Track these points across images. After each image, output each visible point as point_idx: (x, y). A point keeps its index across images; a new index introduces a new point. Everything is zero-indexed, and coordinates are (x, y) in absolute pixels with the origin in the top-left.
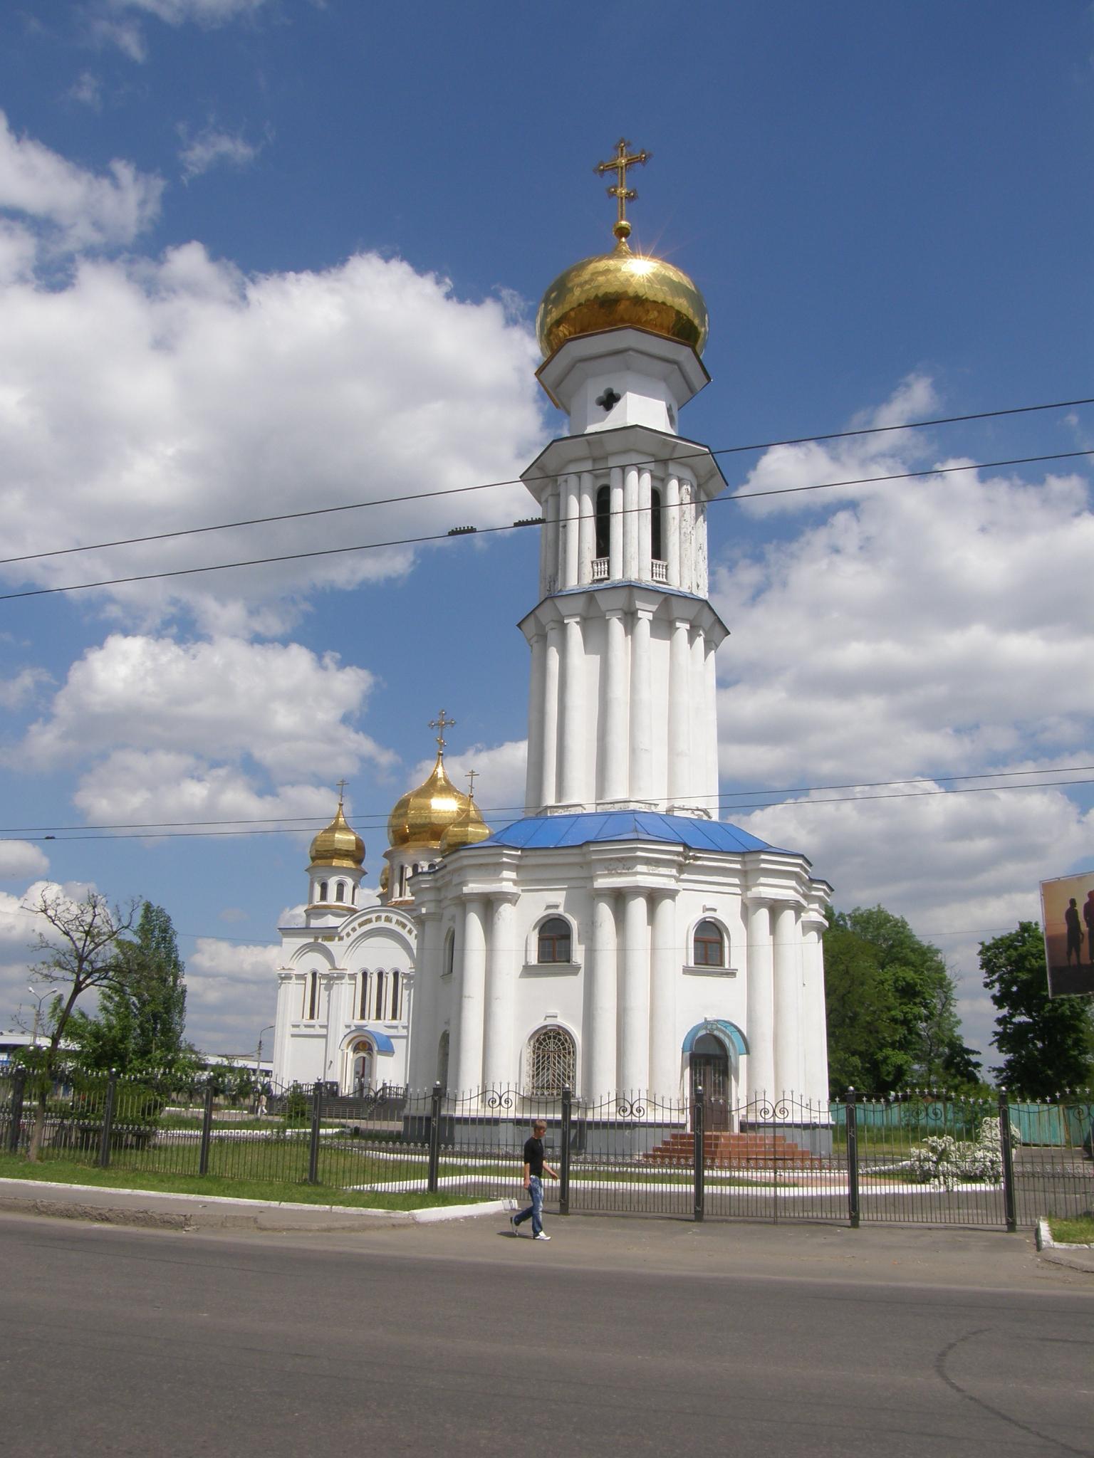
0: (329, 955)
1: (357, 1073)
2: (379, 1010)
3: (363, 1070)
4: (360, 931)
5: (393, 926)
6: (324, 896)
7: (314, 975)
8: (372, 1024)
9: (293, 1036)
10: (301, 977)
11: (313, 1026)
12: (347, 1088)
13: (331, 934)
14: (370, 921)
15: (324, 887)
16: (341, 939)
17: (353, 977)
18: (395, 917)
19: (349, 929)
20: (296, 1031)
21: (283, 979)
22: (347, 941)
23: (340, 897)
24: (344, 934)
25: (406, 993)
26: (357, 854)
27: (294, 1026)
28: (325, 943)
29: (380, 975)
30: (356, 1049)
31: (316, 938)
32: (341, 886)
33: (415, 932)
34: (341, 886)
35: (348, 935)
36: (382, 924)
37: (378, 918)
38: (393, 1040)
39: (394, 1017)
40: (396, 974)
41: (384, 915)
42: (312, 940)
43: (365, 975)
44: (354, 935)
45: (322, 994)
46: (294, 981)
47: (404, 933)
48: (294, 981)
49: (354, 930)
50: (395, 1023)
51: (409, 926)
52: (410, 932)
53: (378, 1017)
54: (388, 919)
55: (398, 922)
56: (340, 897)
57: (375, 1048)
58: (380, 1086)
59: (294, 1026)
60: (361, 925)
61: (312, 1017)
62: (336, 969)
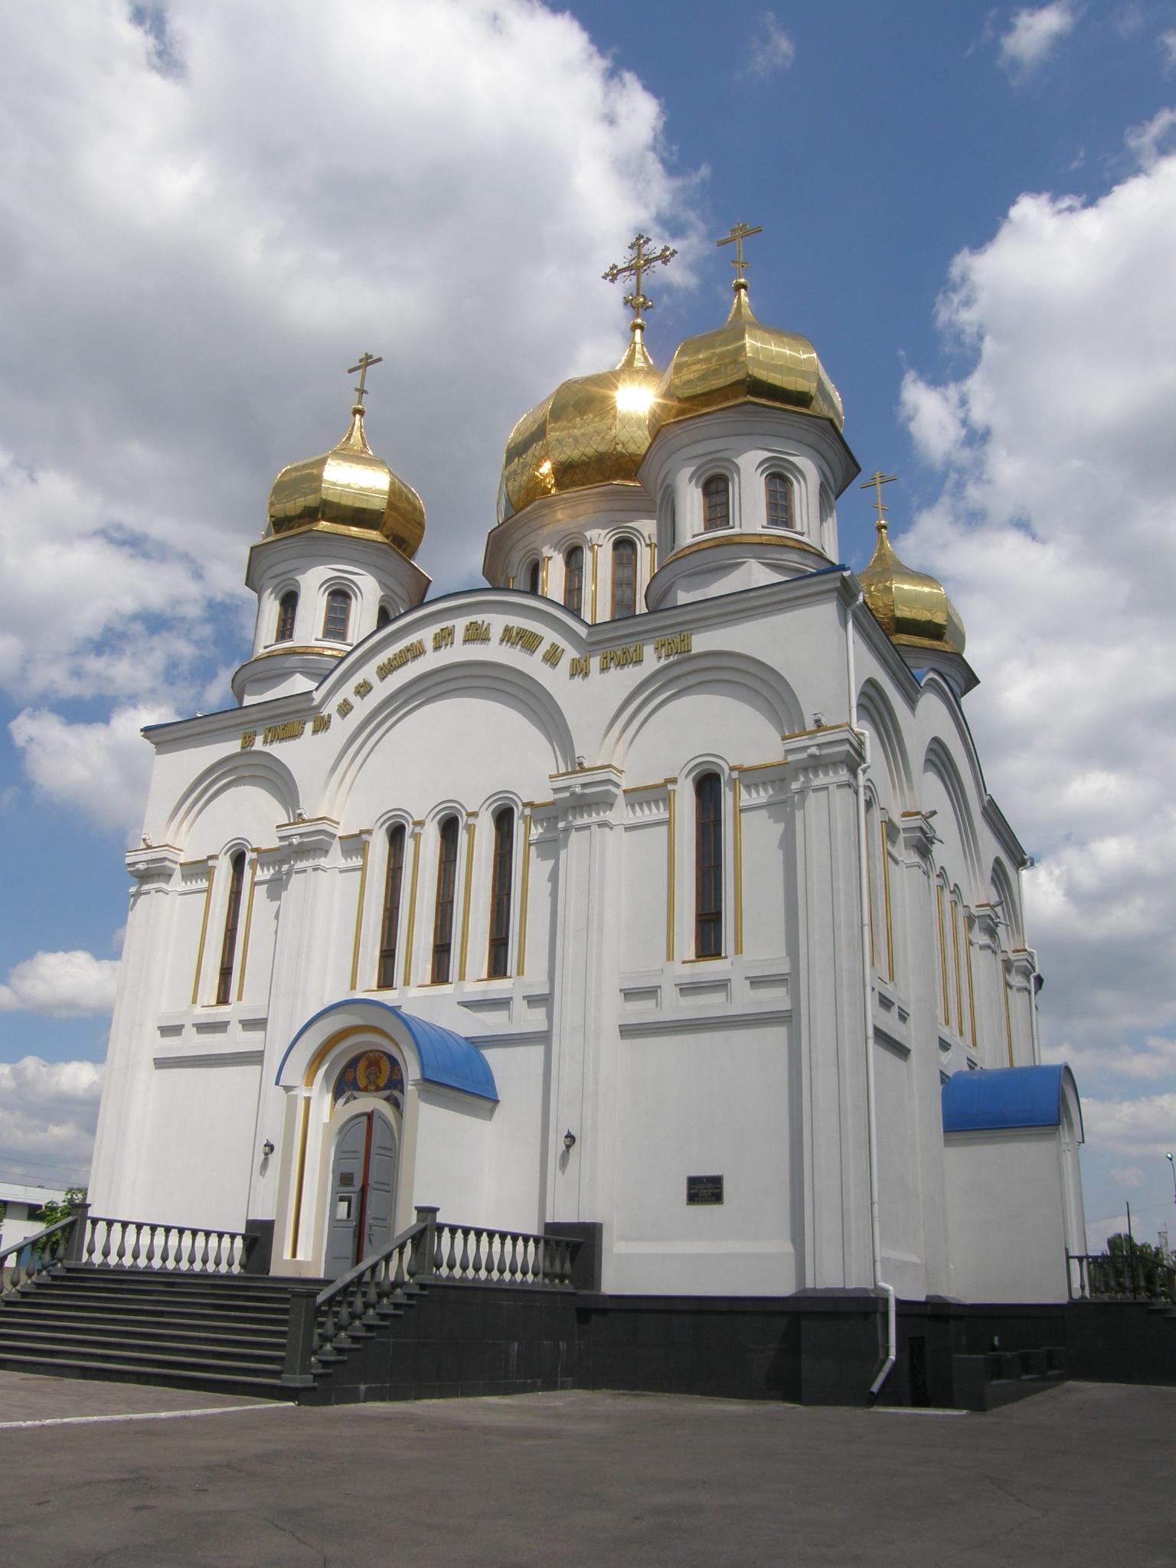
0: (281, 783)
1: (345, 1179)
2: (442, 949)
3: (366, 1174)
4: (382, 690)
5: (494, 652)
6: (285, 630)
7: (238, 861)
8: (415, 996)
9: (161, 1063)
10: (200, 869)
11: (220, 1027)
12: (305, 1252)
13: (291, 717)
14: (415, 652)
15: (289, 602)
16: (322, 725)
17: (356, 844)
18: (497, 623)
19: (347, 691)
20: (175, 1046)
21: (145, 876)
22: (341, 728)
23: (336, 626)
24: (331, 709)
25: (540, 868)
26: (396, 530)
27: (171, 1031)
28: (277, 750)
29: (449, 827)
30: (343, 1086)
31: (248, 740)
32: (340, 595)
33: (571, 653)
34: (340, 595)
35: (345, 709)
36: (459, 652)
37: (444, 639)
38: (494, 1057)
39: (498, 968)
40: (504, 818)
41: (460, 624)
42: (234, 746)
43: (396, 834)
44: (362, 708)
45: (258, 905)
46: (177, 884)
47: (532, 665)
48: (177, 884)
49: (364, 689)
50: (499, 987)
51: (550, 636)
52: (552, 657)
53: (440, 976)
54: (477, 634)
55: (510, 636)
56: (336, 626)
57: (412, 1072)
58: (407, 1221)
59: (171, 1031)
60: (384, 672)
61: (223, 999)
62: (300, 819)
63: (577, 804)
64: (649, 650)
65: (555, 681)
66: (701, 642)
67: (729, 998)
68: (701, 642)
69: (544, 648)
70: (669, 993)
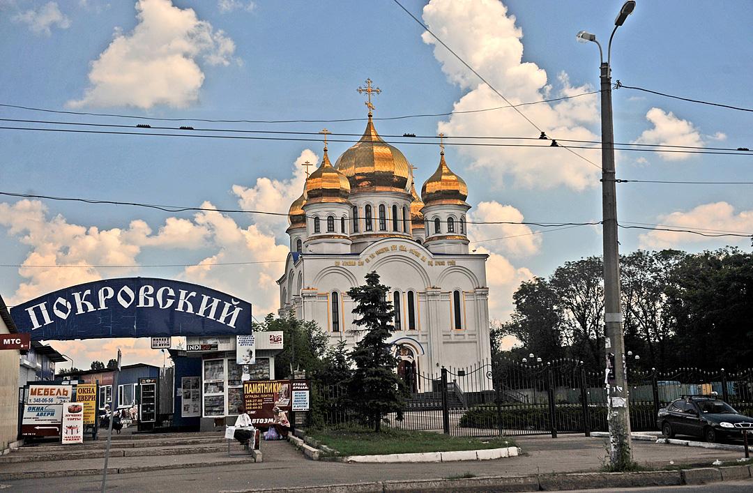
5: (407, 254)
39: (412, 327)
40: (411, 294)
41: (398, 244)
47: (418, 260)
49: (372, 256)
55: (411, 251)
60: (378, 253)
63: (432, 293)
64: (446, 262)
65: (425, 265)
66: (459, 263)
67: (464, 338)
68: (458, 263)
69: (421, 257)
70: (453, 336)
